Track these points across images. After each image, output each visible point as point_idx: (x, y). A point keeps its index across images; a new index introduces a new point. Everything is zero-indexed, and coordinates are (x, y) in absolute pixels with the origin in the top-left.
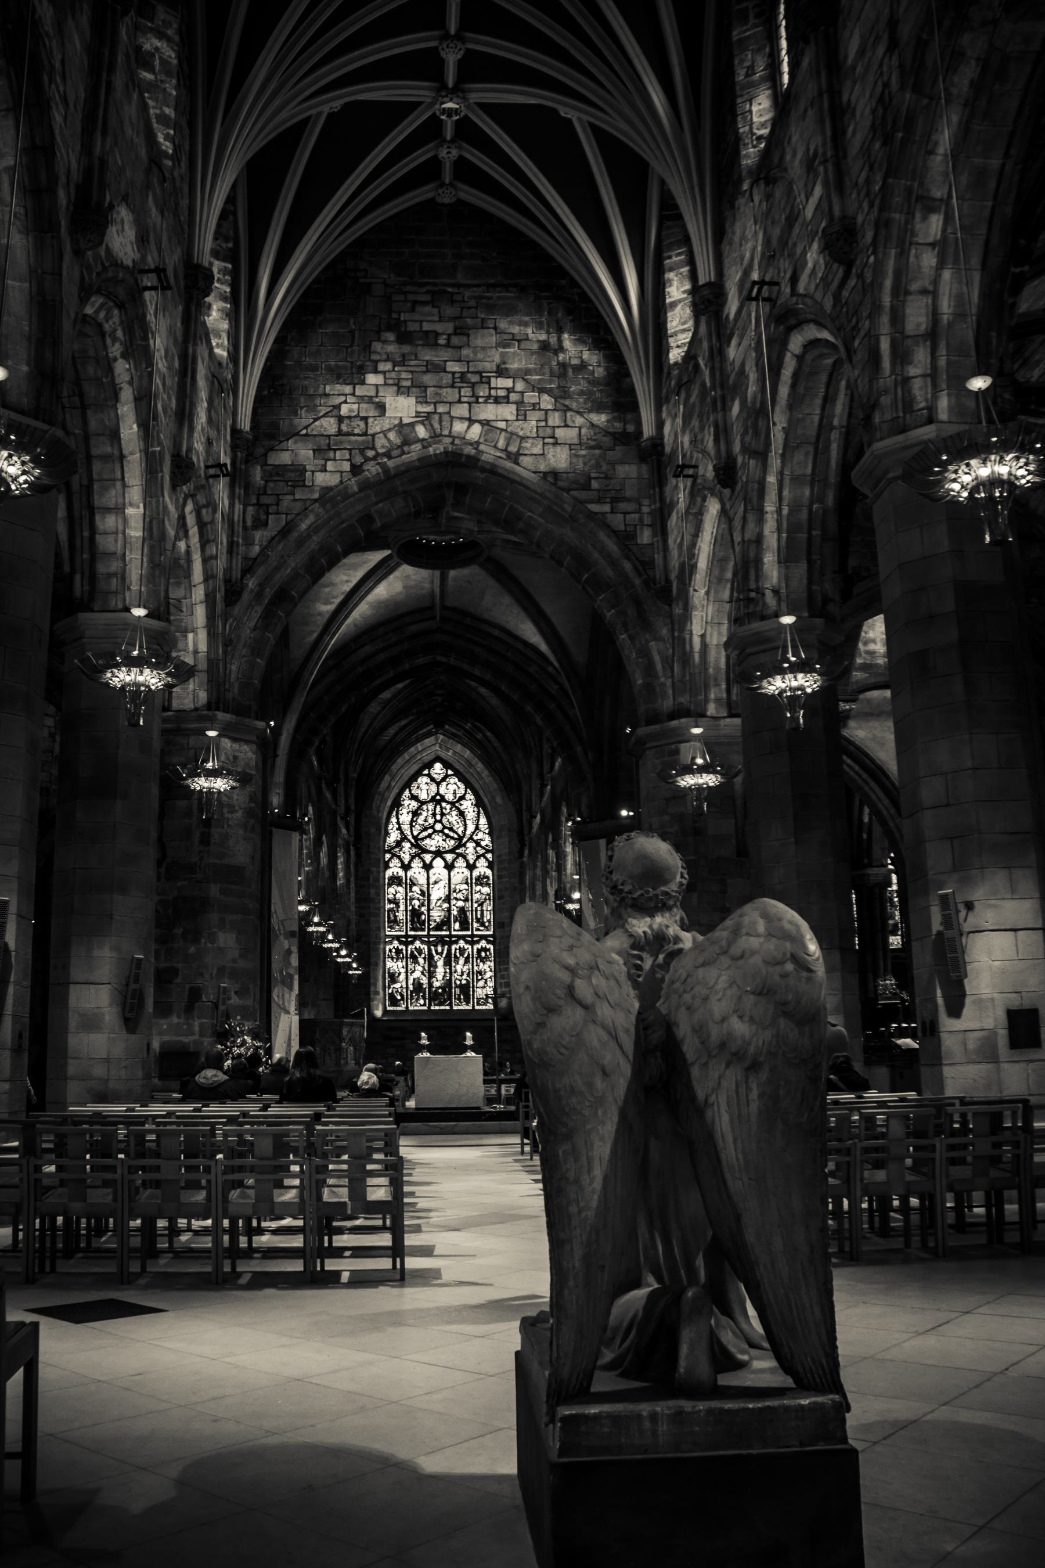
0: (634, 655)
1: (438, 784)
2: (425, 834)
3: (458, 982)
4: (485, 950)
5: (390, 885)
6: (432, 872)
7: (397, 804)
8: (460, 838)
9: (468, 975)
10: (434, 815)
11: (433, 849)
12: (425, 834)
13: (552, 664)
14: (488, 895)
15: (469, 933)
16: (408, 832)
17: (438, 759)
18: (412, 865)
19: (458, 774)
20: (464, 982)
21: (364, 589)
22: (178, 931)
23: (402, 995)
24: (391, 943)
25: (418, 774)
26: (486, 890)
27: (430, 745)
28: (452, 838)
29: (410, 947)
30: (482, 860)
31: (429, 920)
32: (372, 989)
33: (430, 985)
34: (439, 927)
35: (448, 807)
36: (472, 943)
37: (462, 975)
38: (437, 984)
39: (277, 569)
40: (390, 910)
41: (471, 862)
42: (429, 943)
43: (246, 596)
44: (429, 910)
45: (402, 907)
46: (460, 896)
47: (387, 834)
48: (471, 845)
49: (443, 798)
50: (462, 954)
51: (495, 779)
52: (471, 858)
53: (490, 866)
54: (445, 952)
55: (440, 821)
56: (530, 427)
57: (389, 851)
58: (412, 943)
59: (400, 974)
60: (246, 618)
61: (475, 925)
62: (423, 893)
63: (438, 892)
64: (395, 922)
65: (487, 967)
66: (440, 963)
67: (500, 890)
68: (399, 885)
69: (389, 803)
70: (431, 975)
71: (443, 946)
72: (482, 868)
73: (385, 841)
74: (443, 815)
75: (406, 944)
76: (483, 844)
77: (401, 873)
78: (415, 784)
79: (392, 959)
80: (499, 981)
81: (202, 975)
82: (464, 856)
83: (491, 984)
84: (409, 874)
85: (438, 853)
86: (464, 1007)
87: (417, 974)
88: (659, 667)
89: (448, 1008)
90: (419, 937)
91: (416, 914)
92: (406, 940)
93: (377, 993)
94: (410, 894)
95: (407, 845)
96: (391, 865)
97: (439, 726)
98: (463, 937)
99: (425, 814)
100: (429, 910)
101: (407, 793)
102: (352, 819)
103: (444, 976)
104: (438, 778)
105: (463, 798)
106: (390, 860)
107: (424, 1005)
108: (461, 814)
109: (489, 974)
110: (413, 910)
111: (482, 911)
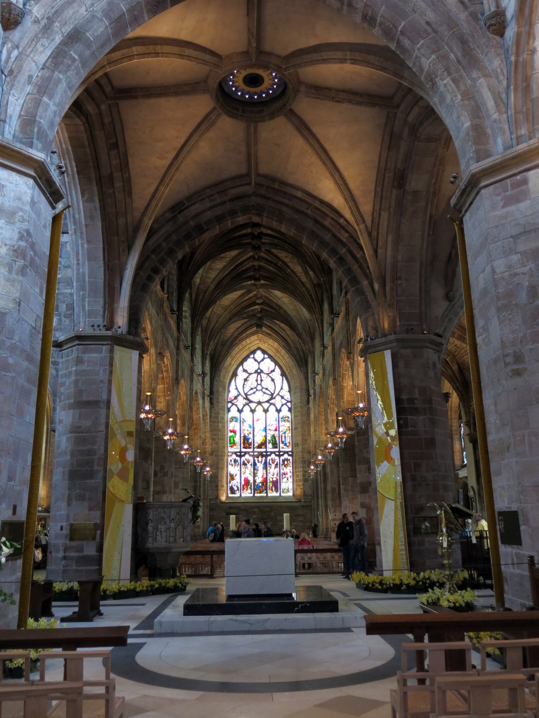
0: (459, 97)
1: (259, 363)
3: (271, 480)
4: (287, 460)
5: (231, 421)
6: (255, 414)
7: (235, 375)
8: (272, 394)
10: (257, 381)
11: (257, 401)
13: (341, 216)
14: (289, 427)
15: (277, 450)
17: (259, 348)
18: (244, 409)
19: (270, 357)
20: (274, 479)
21: (191, 143)
25: (247, 357)
27: (254, 341)
28: (268, 394)
29: (243, 459)
31: (254, 442)
32: (220, 484)
33: (255, 481)
35: (266, 376)
36: (279, 456)
37: (273, 475)
42: (253, 456)
43: (28, 22)
47: (229, 391)
48: (278, 398)
49: (262, 371)
51: (292, 360)
53: (290, 410)
54: (263, 461)
57: (230, 402)
58: (244, 456)
59: (236, 475)
60: (29, 50)
61: (282, 445)
62: (250, 427)
63: (259, 426)
64: (234, 444)
65: (289, 470)
67: (295, 424)
68: (236, 421)
69: (231, 374)
70: (255, 475)
71: (262, 457)
72: (285, 412)
73: (228, 396)
74: (262, 380)
75: (240, 456)
76: (285, 398)
77: (237, 415)
78: (245, 364)
79: (232, 465)
80: (295, 478)
83: (291, 480)
85: (259, 403)
88: (490, 104)
89: (265, 495)
90: (248, 453)
92: (240, 455)
93: (223, 486)
95: (240, 398)
96: (231, 409)
97: (259, 326)
98: (274, 453)
101: (241, 368)
102: (207, 379)
103: (263, 476)
105: (273, 371)
106: (231, 407)
107: (251, 493)
108: (273, 380)
109: (290, 474)
110: (245, 437)
111: (285, 437)
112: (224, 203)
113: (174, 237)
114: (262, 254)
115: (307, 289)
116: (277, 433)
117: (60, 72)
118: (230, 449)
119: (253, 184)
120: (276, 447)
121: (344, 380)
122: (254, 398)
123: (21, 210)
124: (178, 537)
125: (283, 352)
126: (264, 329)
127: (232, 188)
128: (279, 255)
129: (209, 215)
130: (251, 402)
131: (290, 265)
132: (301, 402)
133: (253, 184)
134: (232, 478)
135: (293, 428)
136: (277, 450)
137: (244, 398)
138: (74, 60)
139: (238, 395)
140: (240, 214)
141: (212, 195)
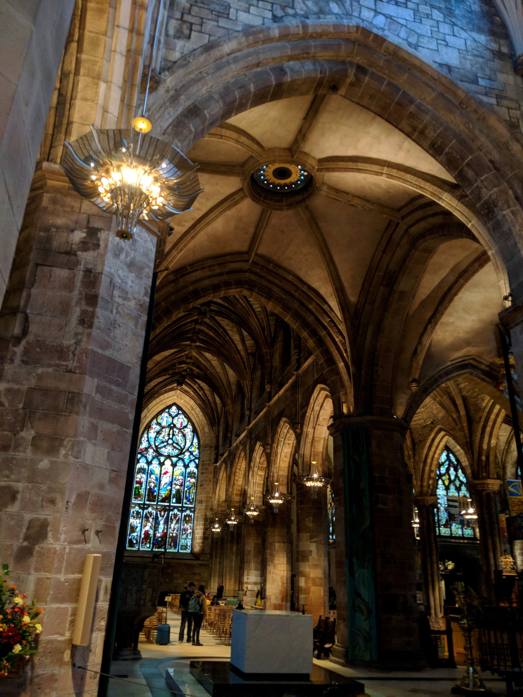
1: (173, 418)
2: (162, 445)
4: (188, 516)
5: (138, 473)
6: (163, 467)
7: (148, 427)
8: (182, 449)
9: (177, 531)
10: (169, 435)
11: (166, 454)
12: (162, 445)
13: (327, 303)
15: (180, 505)
16: (153, 443)
19: (184, 413)
20: (174, 535)
22: (28, 434)
23: (137, 541)
24: (134, 507)
25: (163, 411)
26: (193, 480)
28: (178, 449)
29: (145, 511)
30: (193, 463)
31: (158, 496)
33: (155, 535)
34: (163, 500)
35: (177, 431)
36: (182, 511)
37: (174, 530)
38: (158, 535)
39: (195, 81)
40: (136, 488)
41: (187, 463)
42: (157, 509)
44: (159, 489)
45: (144, 486)
46: (178, 482)
47: (141, 443)
48: (187, 454)
49: (175, 426)
50: (175, 518)
52: (187, 461)
53: (197, 467)
55: (172, 439)
56: (425, 28)
57: (140, 453)
58: (147, 508)
59: (137, 527)
63: (166, 480)
64: (138, 496)
66: (162, 522)
68: (144, 473)
70: (156, 529)
71: (165, 512)
72: (192, 468)
74: (173, 435)
75: (144, 509)
76: (194, 454)
77: (146, 466)
78: (160, 417)
79: (134, 517)
81: (53, 502)
82: (183, 460)
83: (190, 537)
84: (151, 467)
85: (169, 457)
86: (173, 550)
87: (147, 528)
89: (163, 550)
90: (152, 505)
91: (151, 491)
92: (144, 507)
94: (149, 479)
95: (151, 451)
96: (140, 461)
97: (180, 384)
99: (163, 434)
100: (159, 489)
101: (155, 421)
103: (163, 530)
104: (174, 414)
106: (140, 458)
107: (149, 547)
108: (184, 436)
110: (150, 489)
112: (221, 274)
113: (173, 298)
114: (207, 320)
115: (241, 356)
116: (182, 488)
117: (179, 141)
118: (134, 501)
119: (250, 262)
120: (180, 503)
121: (279, 447)
122: (165, 451)
123: (148, 266)
124: (147, 600)
125: (198, 410)
126: (184, 386)
127: (232, 262)
128: (221, 322)
129: (207, 282)
130: (162, 455)
131: (230, 333)
132: (210, 460)
133: (250, 262)
134: (133, 529)
135: (199, 485)
136: (180, 505)
137: (154, 451)
138: (191, 132)
139: (149, 447)
140: (234, 287)
141: (213, 266)
